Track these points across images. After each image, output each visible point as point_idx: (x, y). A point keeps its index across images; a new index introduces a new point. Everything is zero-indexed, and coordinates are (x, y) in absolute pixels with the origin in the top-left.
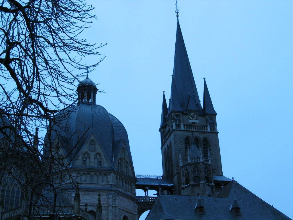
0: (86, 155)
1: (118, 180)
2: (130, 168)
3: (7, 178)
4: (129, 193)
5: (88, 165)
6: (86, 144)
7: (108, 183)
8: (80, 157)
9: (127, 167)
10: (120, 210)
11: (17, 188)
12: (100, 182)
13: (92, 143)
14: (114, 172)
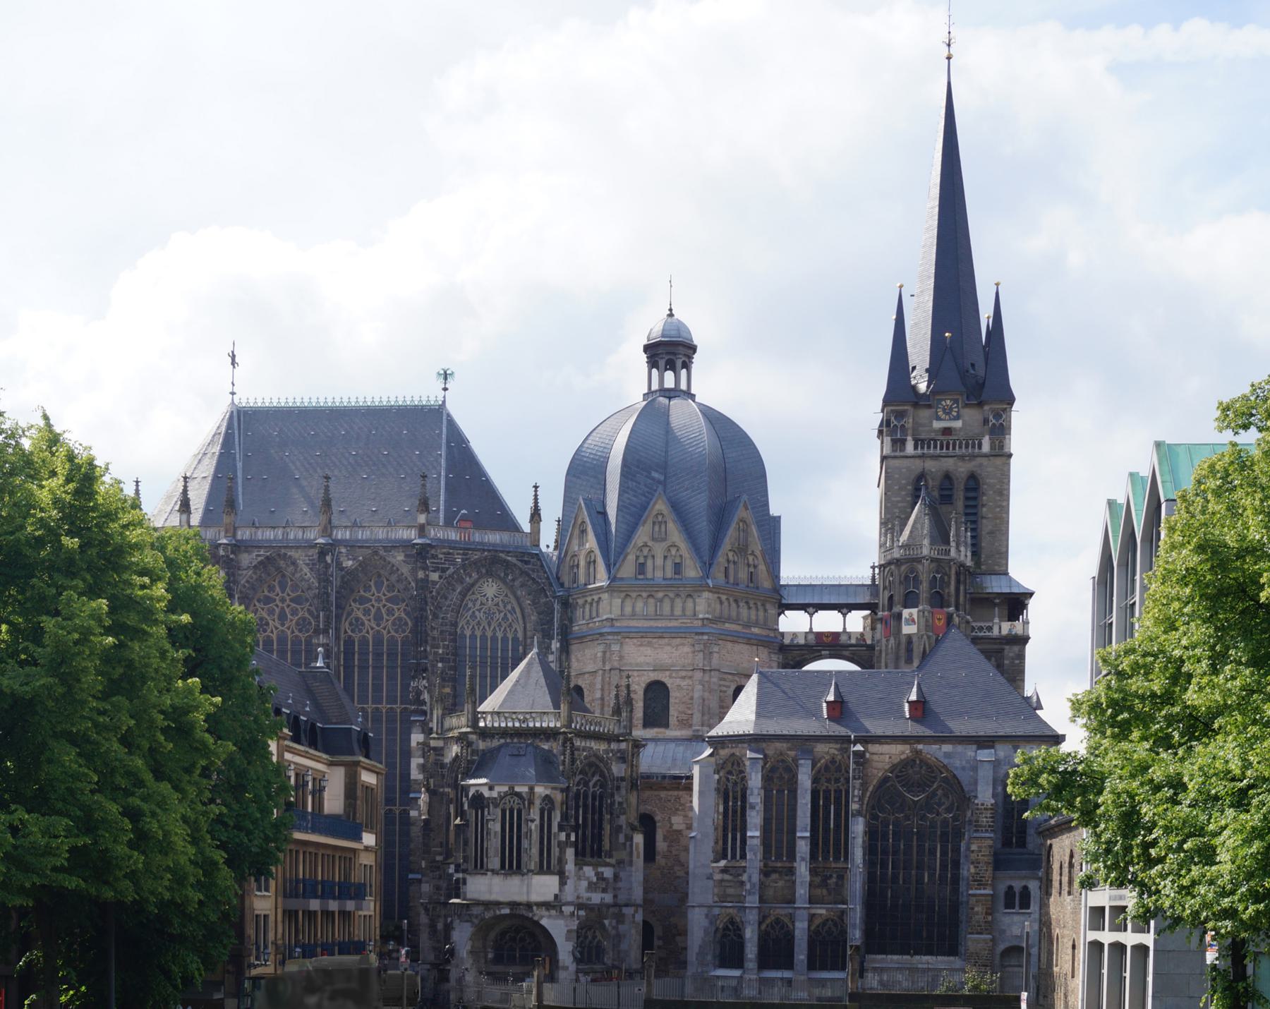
0: (646, 551)
1: (726, 604)
3: (479, 610)
4: (755, 630)
5: (649, 575)
6: (645, 522)
7: (695, 615)
8: (631, 558)
9: (755, 567)
10: (726, 676)
11: (502, 629)
12: (678, 611)
13: (660, 518)
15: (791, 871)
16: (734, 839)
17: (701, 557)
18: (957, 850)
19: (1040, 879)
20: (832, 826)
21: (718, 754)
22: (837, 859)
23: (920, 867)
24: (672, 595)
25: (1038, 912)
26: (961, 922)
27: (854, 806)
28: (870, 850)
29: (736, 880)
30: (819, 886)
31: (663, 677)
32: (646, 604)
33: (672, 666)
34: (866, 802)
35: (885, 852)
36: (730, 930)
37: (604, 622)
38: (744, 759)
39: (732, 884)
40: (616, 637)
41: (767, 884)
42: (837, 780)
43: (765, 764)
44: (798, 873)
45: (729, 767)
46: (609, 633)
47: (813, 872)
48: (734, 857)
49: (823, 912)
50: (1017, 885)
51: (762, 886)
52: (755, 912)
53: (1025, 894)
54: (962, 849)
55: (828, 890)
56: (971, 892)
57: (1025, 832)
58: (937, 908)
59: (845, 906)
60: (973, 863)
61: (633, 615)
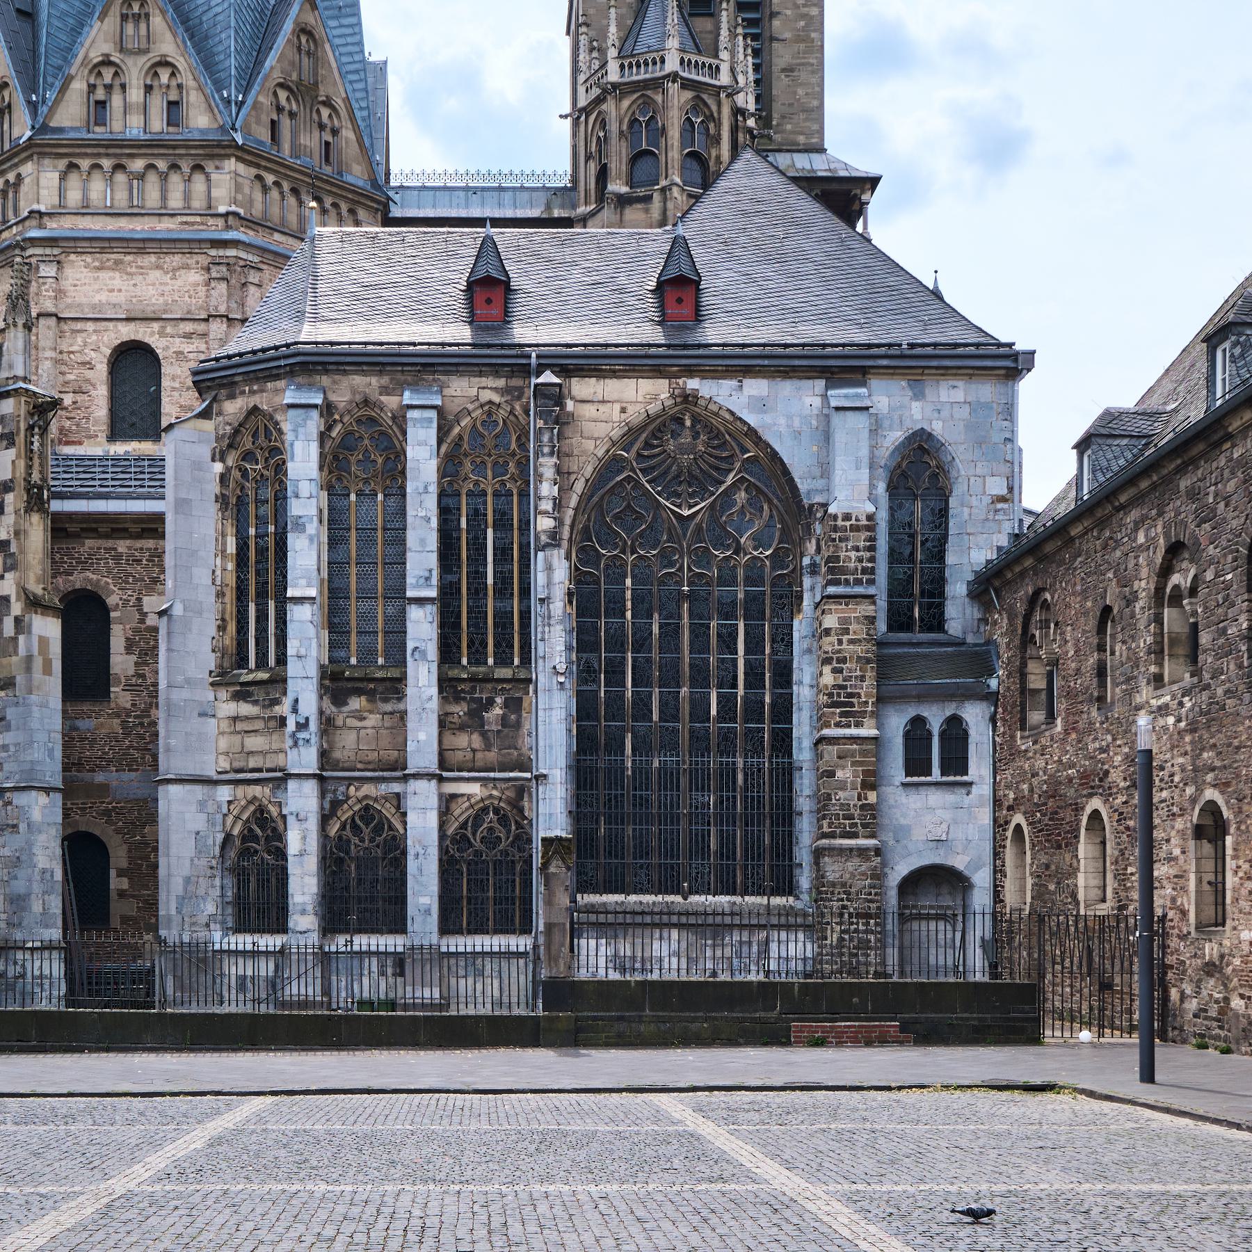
1: (275, 194)
2: (348, 134)
5: (117, 126)
9: (335, 132)
12: (175, 202)
14: (239, 154)
15: (395, 687)
16: (262, 617)
17: (219, 85)
18: (784, 638)
19: (991, 697)
20: (490, 580)
21: (220, 413)
22: (503, 659)
23: (700, 677)
24: (162, 165)
25: (989, 780)
26: (800, 814)
27: (545, 523)
28: (584, 641)
29: (268, 713)
30: (462, 728)
31: (146, 334)
32: (110, 180)
33: (165, 311)
34: (568, 521)
35: (616, 642)
36: (255, 839)
37: (27, 223)
38: (278, 417)
39: (259, 725)
40: (48, 251)
41: (339, 722)
42: (500, 468)
43: (329, 428)
44: (410, 691)
45: (247, 442)
46: (33, 241)
47: (447, 686)
48: (262, 663)
49: (475, 789)
50: (935, 717)
51: (328, 725)
52: (311, 787)
53: (956, 733)
54: (796, 635)
55: (484, 735)
56: (826, 732)
57: (942, 594)
58: (740, 777)
59: (528, 775)
60: (827, 661)
61: (85, 210)
